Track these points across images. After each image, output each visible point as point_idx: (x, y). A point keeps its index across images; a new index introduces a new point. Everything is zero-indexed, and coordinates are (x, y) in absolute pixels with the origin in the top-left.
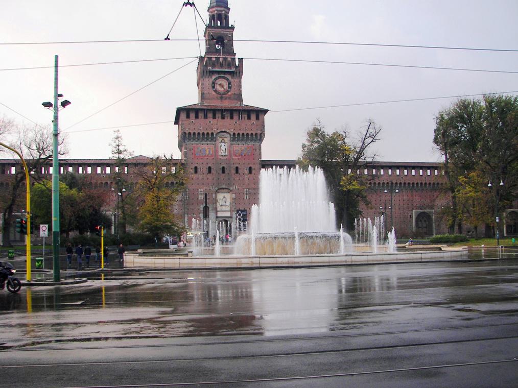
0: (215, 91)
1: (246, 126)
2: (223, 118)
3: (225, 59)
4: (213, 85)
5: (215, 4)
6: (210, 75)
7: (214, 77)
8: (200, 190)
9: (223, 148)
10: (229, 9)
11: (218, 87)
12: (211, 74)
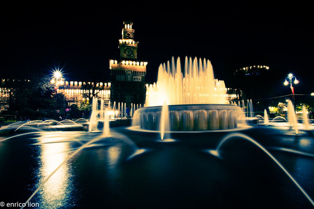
0: (126, 54)
9: (129, 77)
11: (127, 53)
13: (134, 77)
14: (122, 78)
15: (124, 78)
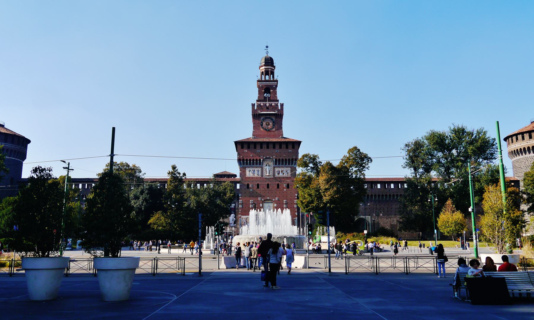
0: (263, 128)
1: (284, 154)
2: (268, 148)
3: (271, 105)
4: (261, 124)
5: (264, 63)
6: (259, 116)
7: (262, 118)
8: (251, 201)
10: (274, 67)
12: (260, 116)
13: (277, 169)
14: (256, 172)
15: (260, 173)
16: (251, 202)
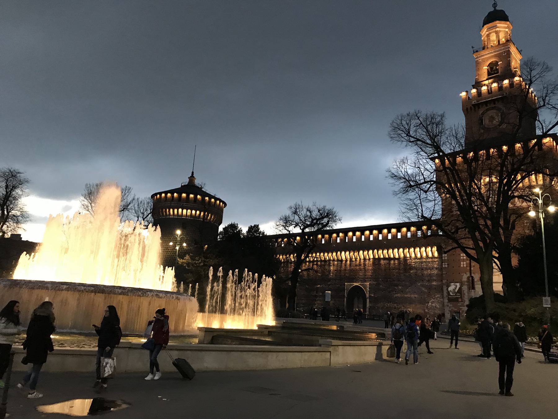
4: (480, 122)
6: (475, 111)
12: (477, 108)
16: (462, 258)
